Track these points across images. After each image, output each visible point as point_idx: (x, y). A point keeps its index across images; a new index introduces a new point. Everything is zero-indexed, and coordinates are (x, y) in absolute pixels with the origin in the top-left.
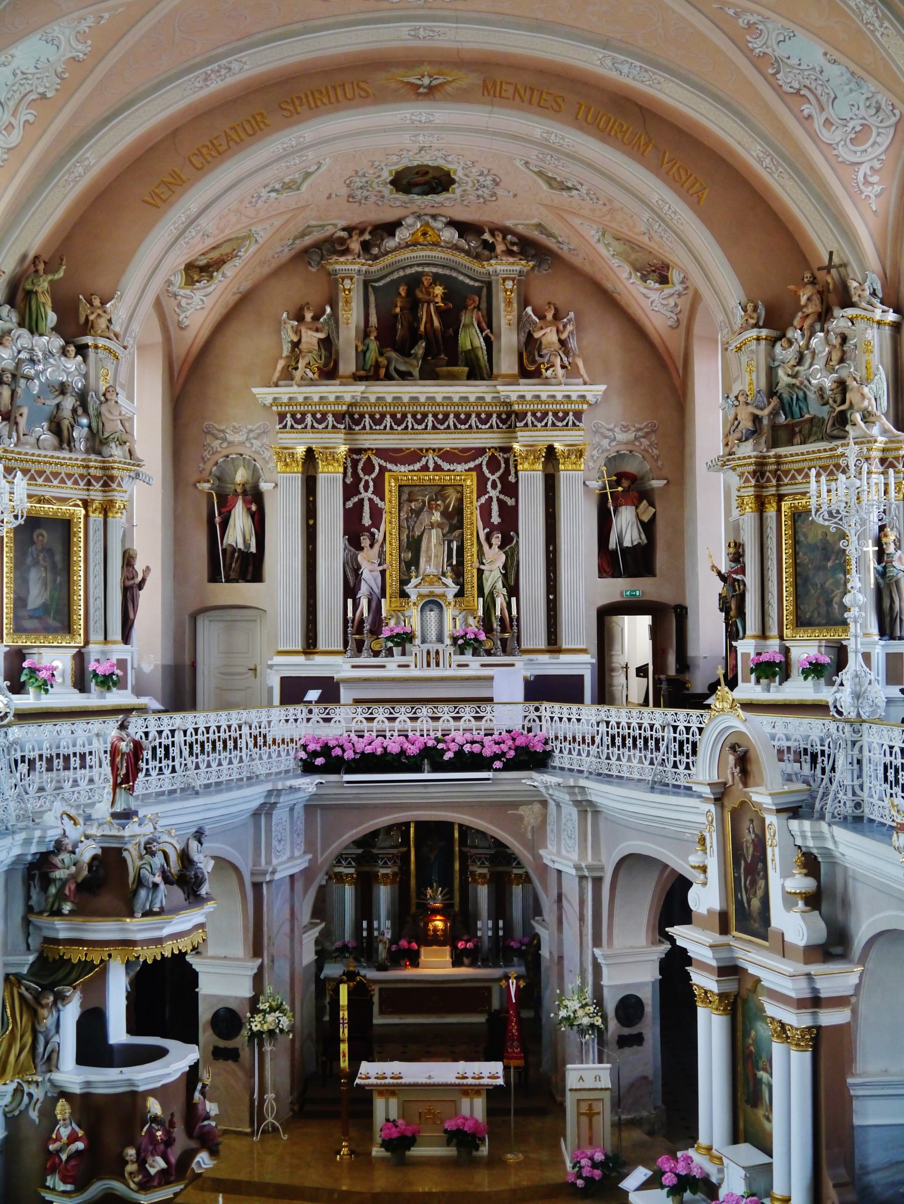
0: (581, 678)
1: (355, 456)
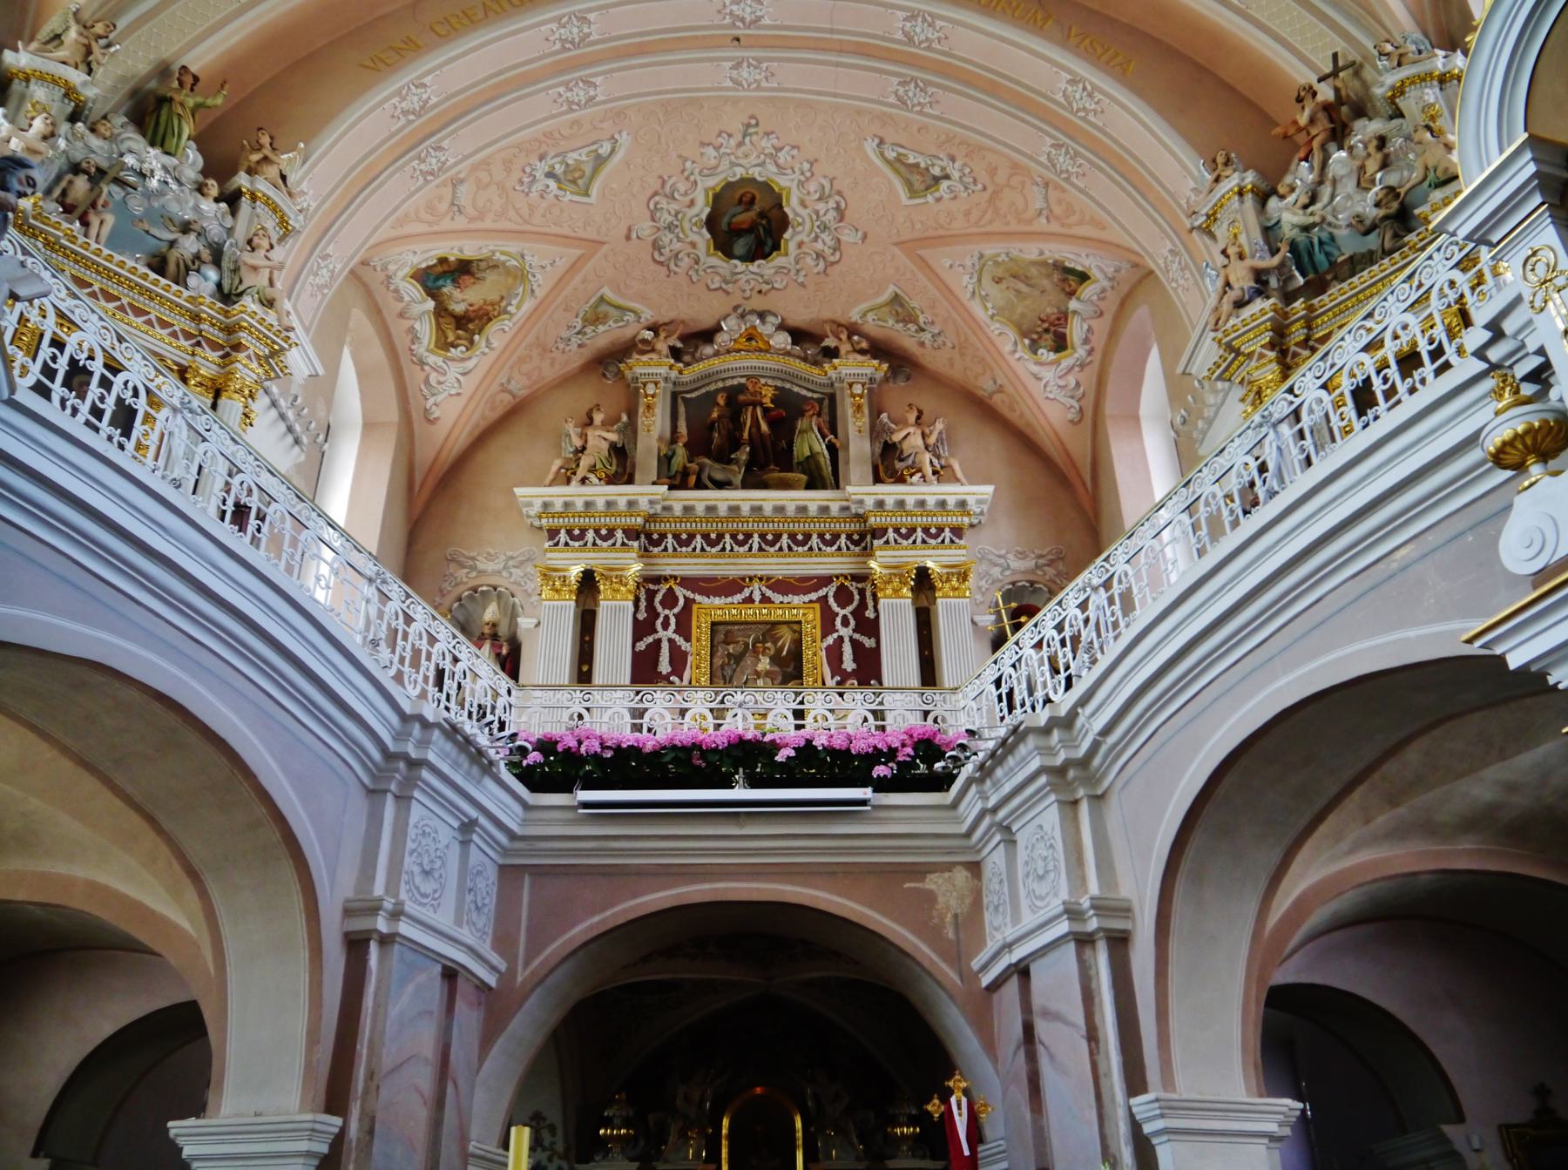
1: (651, 587)
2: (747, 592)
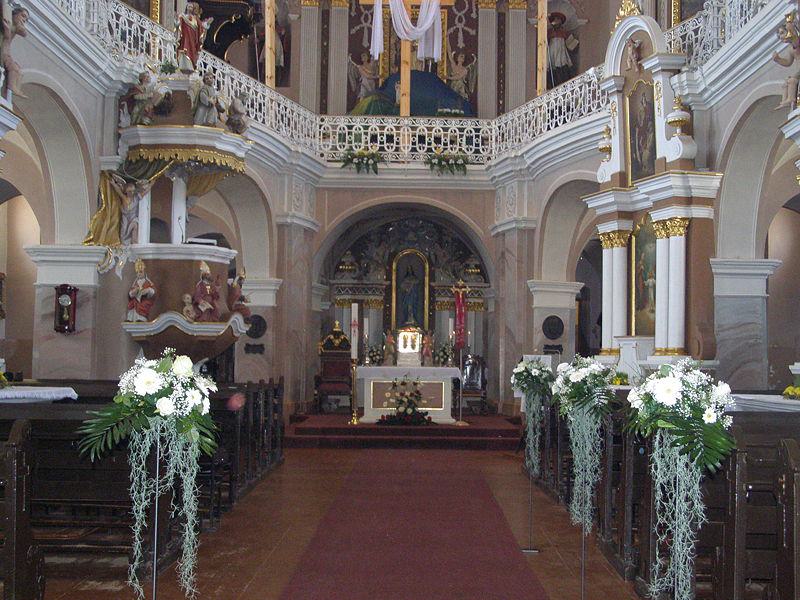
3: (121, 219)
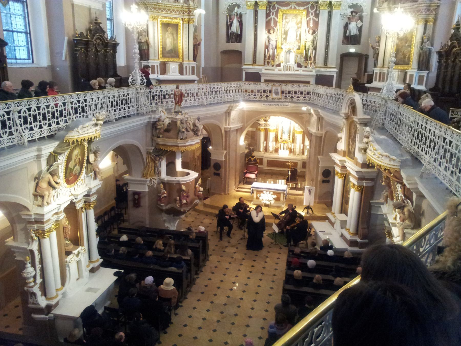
0: (333, 76)
2: (291, 6)
3: (155, 169)
